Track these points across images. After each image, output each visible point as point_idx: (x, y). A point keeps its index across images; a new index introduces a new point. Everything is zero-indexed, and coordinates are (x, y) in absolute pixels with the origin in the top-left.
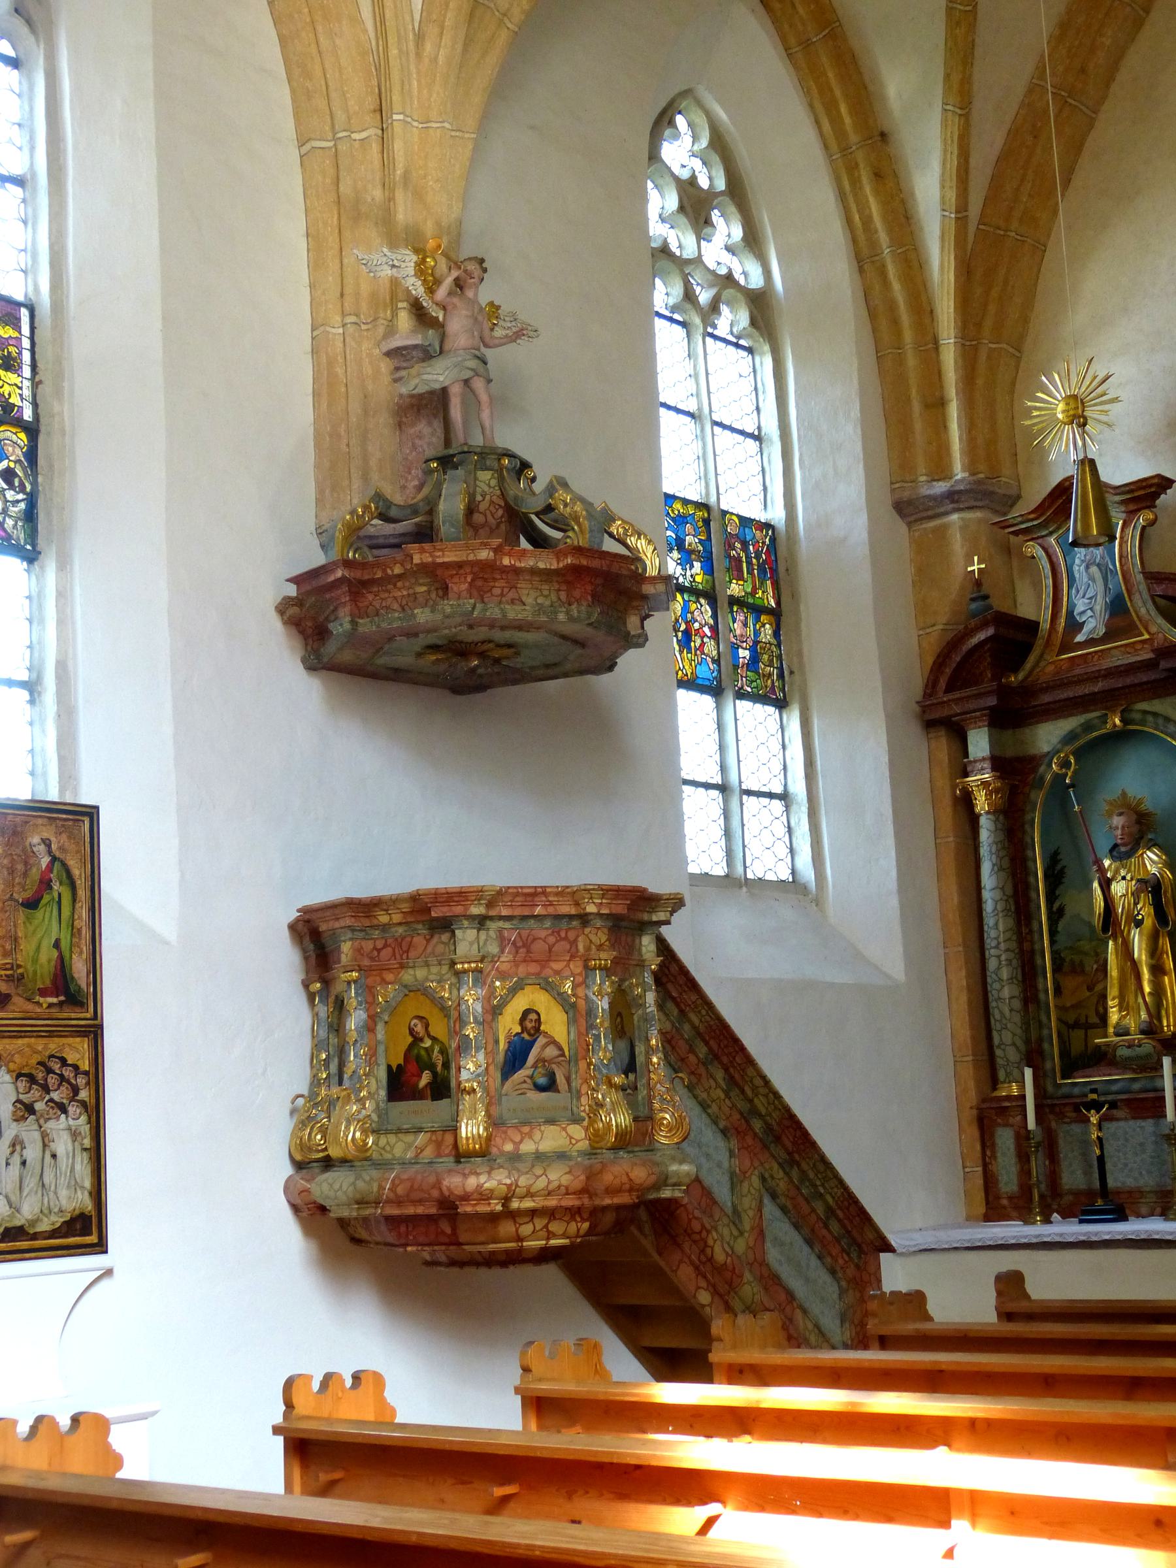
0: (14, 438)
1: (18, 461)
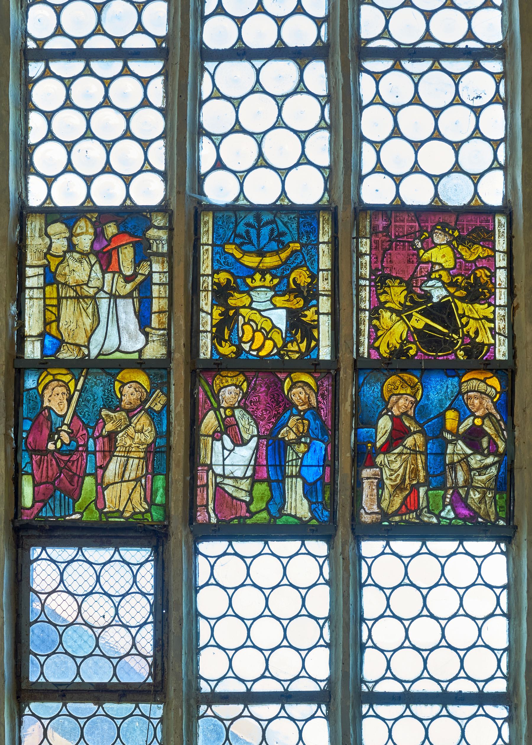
0: (482, 387)
1: (489, 415)
